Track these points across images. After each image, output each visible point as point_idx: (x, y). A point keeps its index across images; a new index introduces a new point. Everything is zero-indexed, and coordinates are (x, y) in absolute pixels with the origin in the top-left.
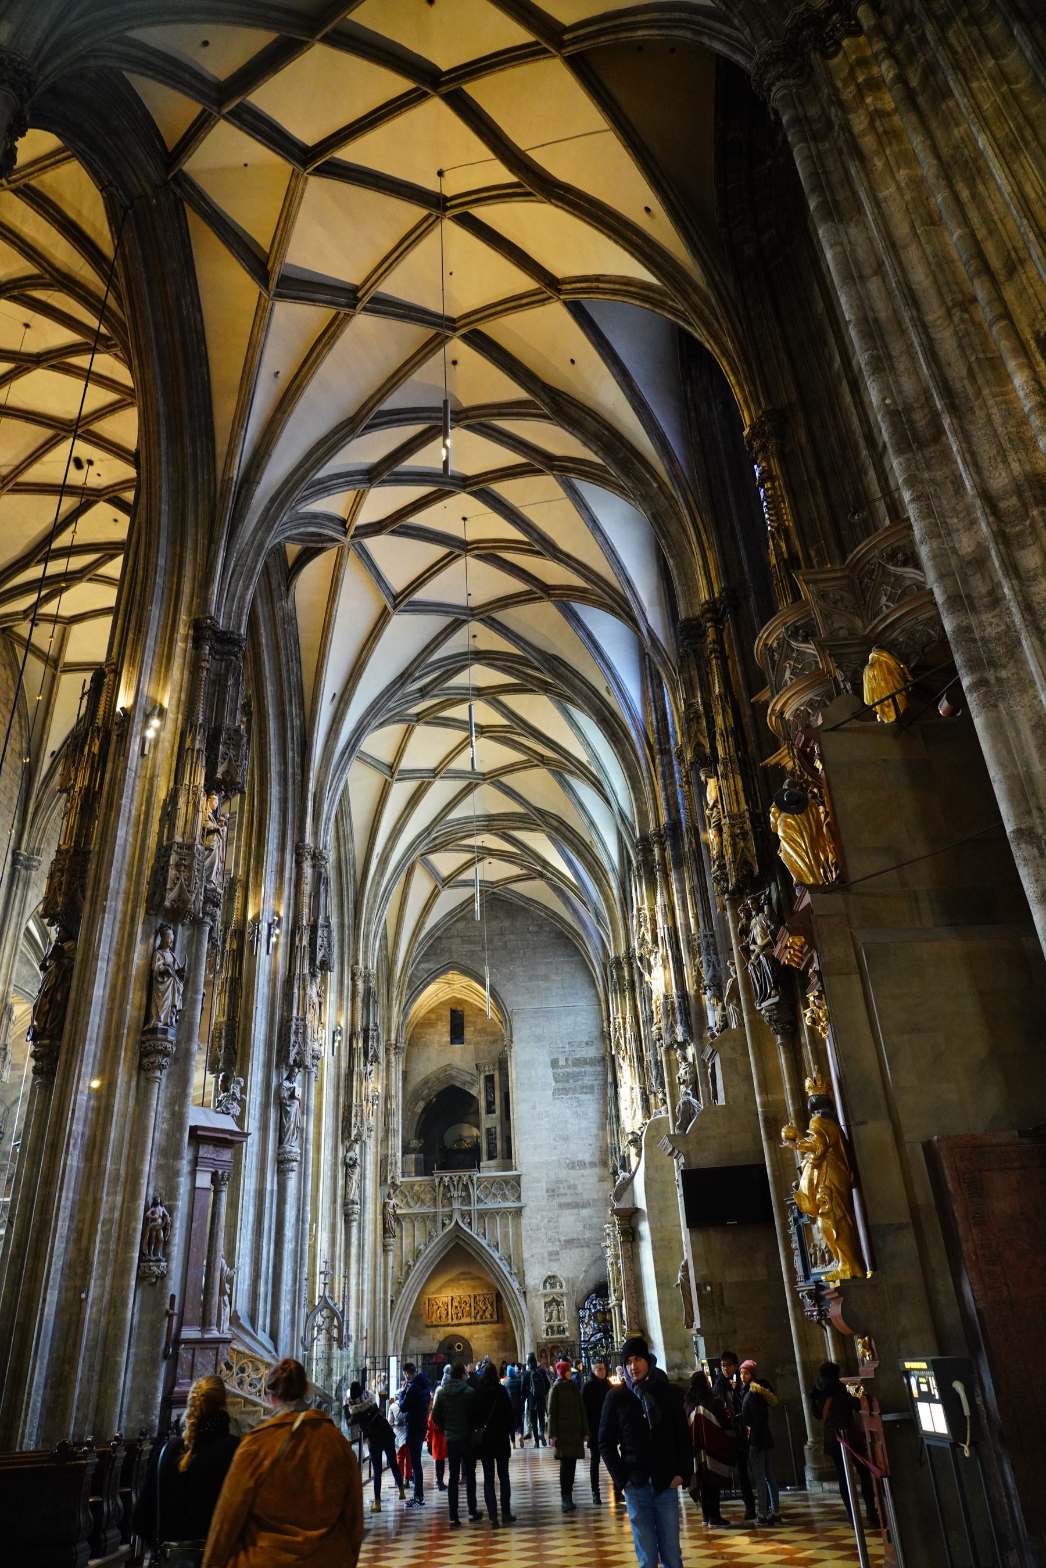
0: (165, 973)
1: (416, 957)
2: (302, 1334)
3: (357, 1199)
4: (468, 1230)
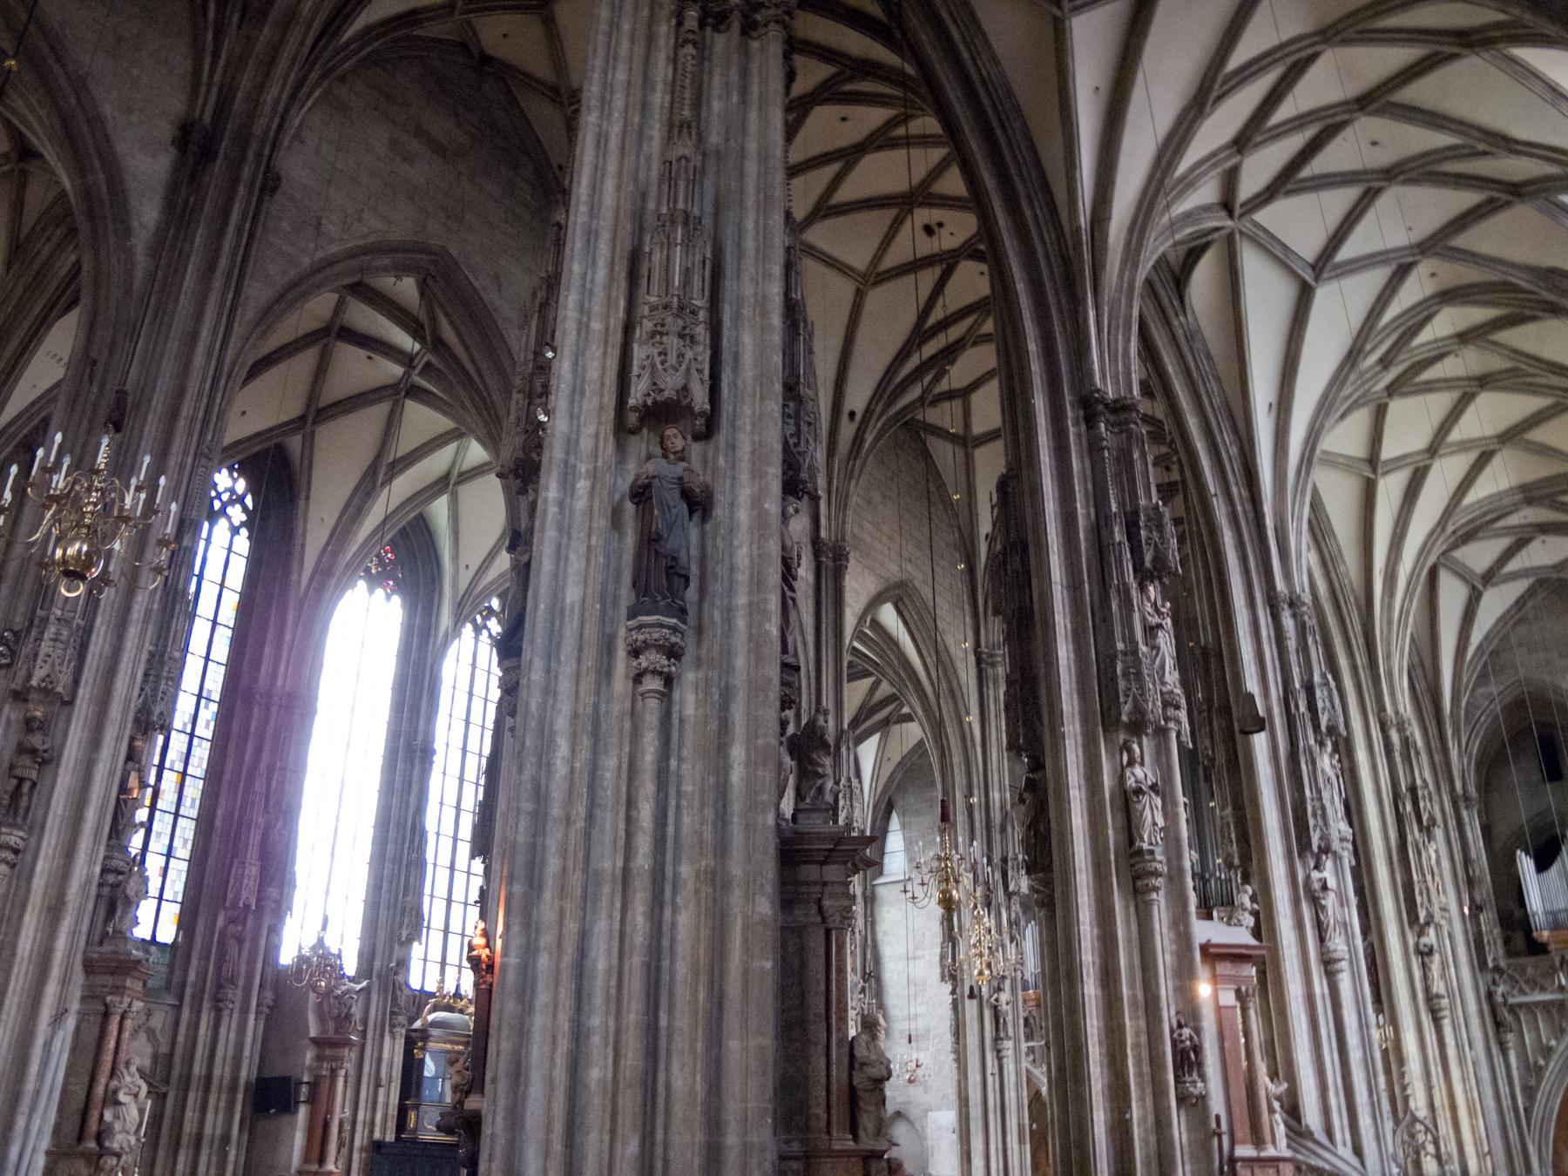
0: (1139, 791)
1: (1469, 681)
2: (1391, 1149)
3: (1442, 991)
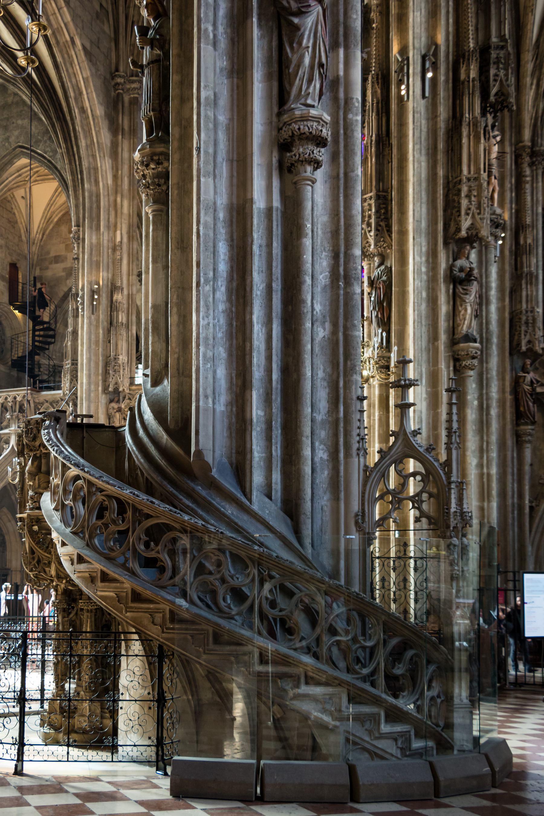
2: (355, 506)
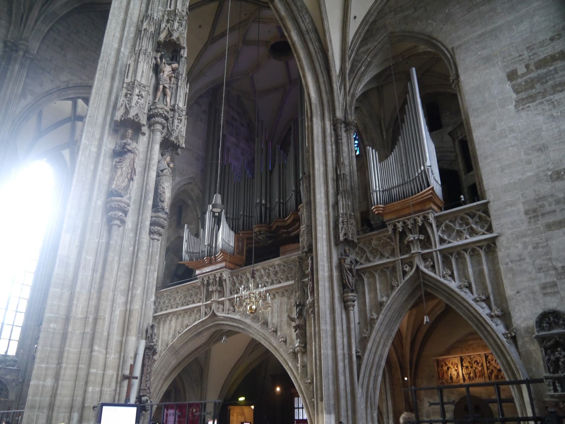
4: (432, 274)
